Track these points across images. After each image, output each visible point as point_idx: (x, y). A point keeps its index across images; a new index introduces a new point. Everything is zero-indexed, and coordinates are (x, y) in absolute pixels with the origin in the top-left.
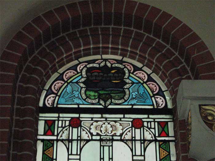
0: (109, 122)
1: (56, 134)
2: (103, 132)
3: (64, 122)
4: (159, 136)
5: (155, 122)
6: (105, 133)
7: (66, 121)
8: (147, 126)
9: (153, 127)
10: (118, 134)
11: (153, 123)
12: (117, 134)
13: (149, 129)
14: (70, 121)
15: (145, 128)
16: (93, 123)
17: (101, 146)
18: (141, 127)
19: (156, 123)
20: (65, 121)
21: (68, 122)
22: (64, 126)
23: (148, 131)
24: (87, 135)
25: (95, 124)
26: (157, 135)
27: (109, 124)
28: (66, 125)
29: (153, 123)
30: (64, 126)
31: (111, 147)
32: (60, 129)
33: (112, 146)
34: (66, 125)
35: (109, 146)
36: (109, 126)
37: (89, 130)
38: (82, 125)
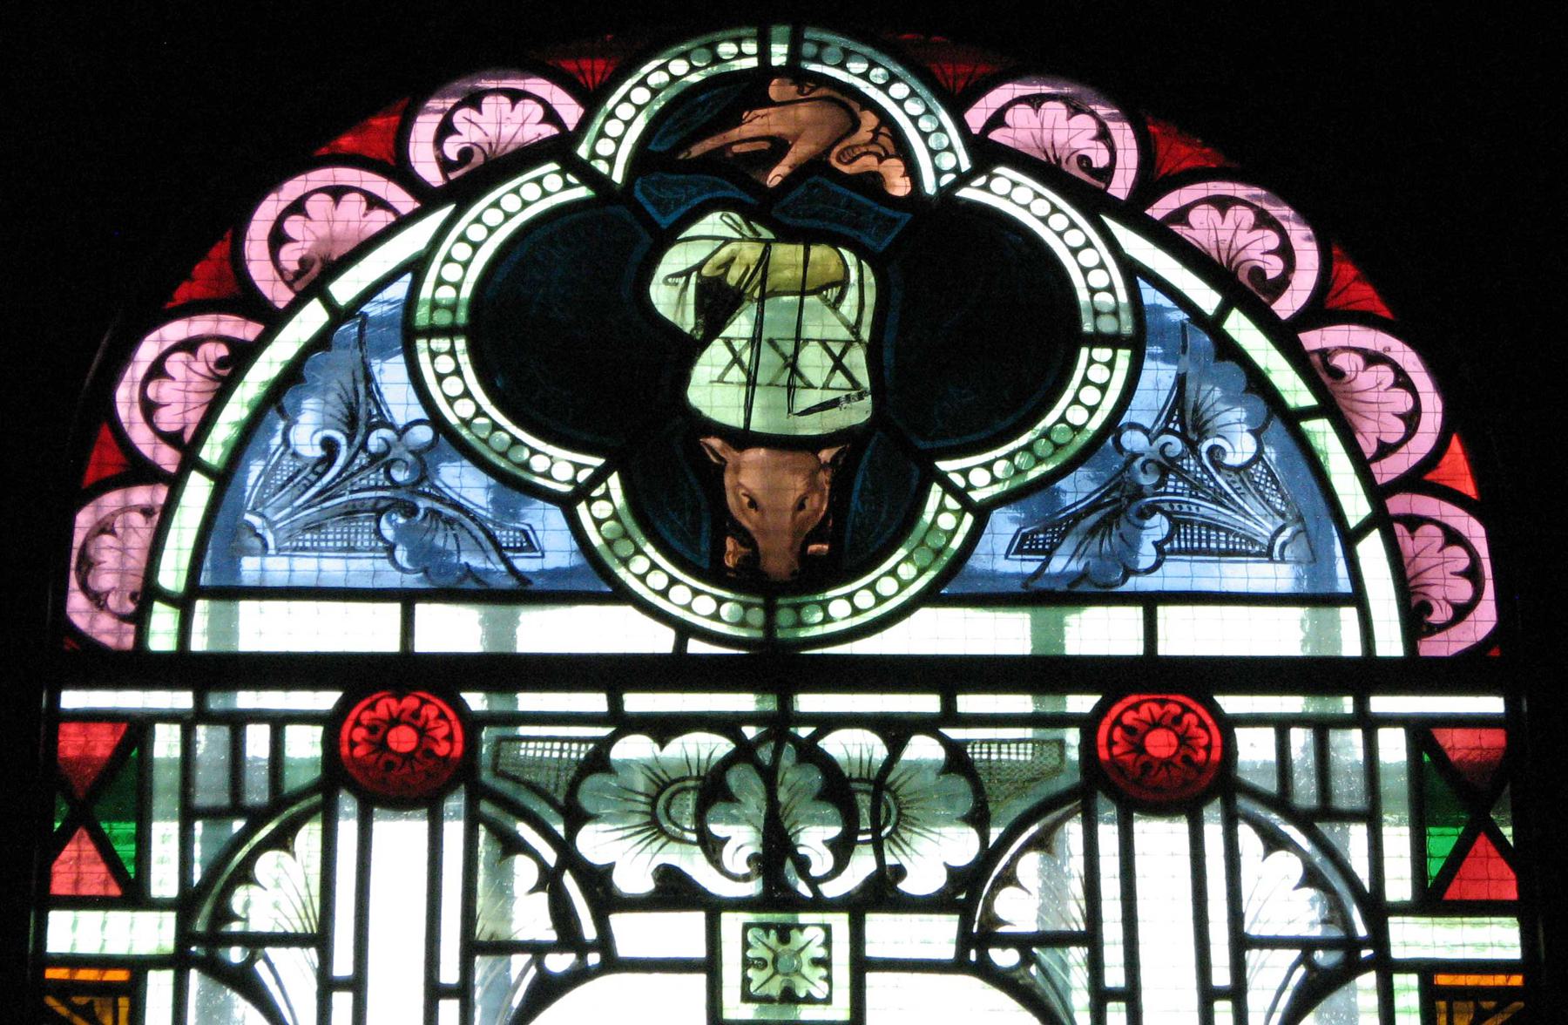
0: (804, 732)
1: (164, 881)
7: (292, 732)
8: (1270, 785)
10: (923, 878)
12: (907, 886)
13: (1306, 821)
14: (331, 723)
15: (1243, 803)
18: (1205, 799)
20: (278, 722)
26: (1399, 888)
38: (486, 776)
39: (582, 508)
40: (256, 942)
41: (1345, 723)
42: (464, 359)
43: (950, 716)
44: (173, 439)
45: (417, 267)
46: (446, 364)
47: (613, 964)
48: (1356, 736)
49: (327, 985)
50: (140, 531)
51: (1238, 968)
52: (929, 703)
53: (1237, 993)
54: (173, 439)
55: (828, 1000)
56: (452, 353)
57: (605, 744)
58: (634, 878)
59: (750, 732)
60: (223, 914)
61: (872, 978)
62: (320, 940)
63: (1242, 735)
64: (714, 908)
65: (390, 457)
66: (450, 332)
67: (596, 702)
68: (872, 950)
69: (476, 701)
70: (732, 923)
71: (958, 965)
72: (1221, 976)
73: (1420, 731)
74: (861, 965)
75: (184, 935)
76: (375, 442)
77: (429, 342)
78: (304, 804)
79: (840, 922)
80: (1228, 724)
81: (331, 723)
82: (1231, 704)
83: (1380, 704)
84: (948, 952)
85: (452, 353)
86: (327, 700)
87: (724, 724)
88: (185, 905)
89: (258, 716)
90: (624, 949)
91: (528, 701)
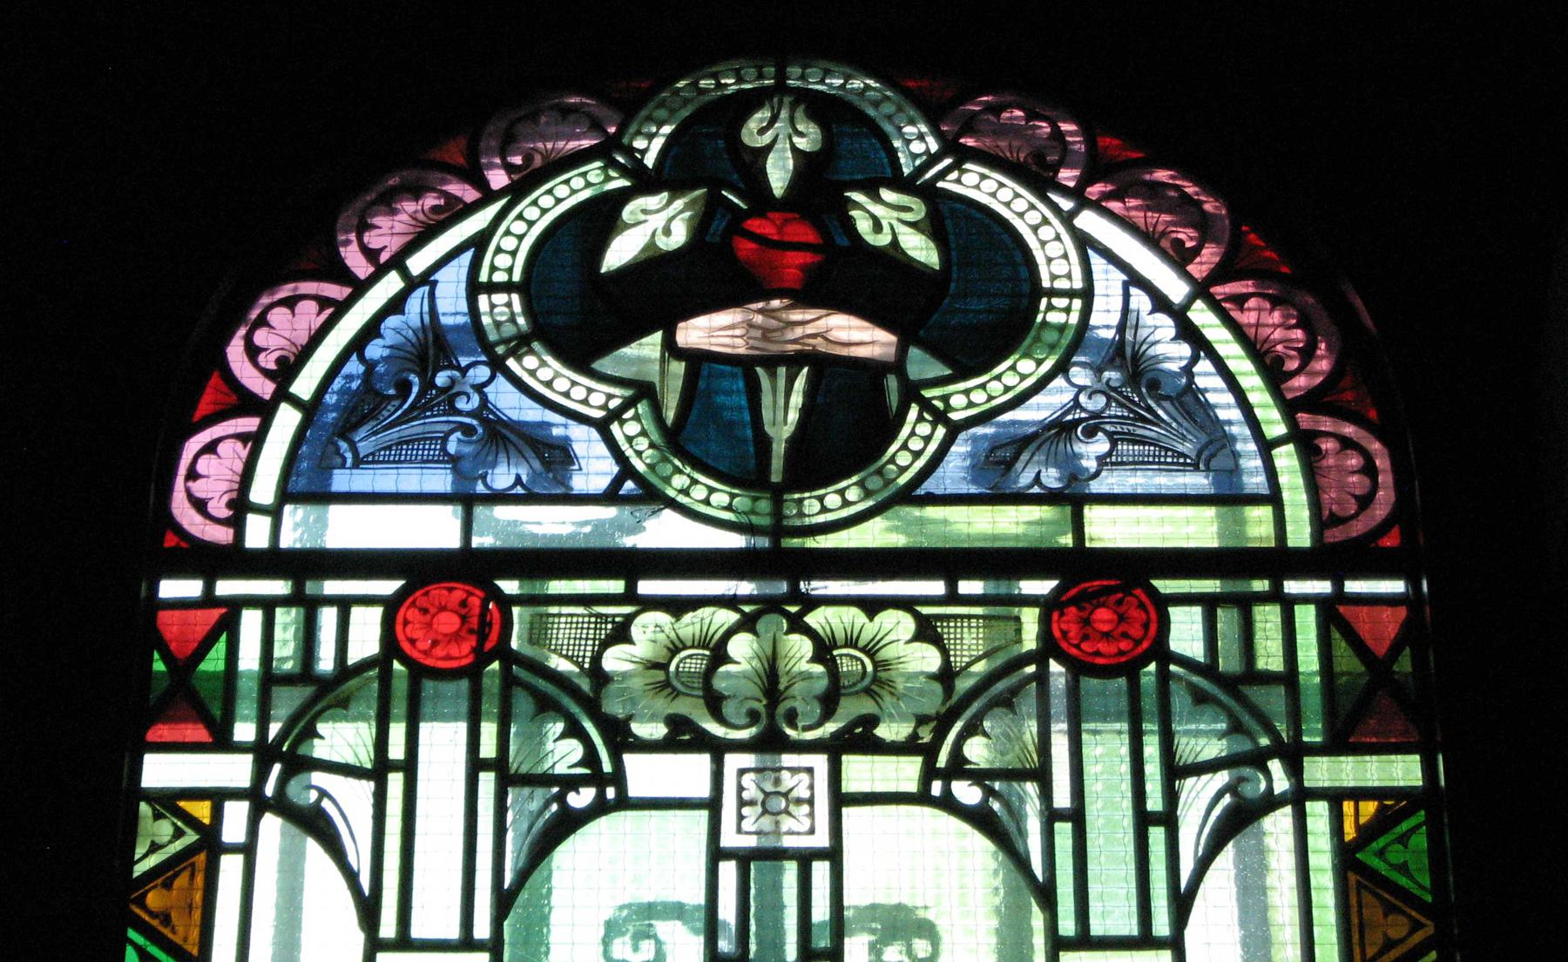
1: (244, 731)
3: (328, 618)
4: (1337, 745)
5: (1288, 604)
6: (754, 717)
7: (357, 612)
9: (1270, 657)
11: (1268, 618)
14: (391, 605)
17: (716, 854)
19: (1306, 617)
20: (344, 604)
21: (377, 612)
28: (353, 657)
30: (326, 662)
31: (821, 870)
32: (286, 702)
33: (834, 854)
34: (353, 657)
35: (805, 859)
39: (615, 428)
41: (1263, 598)
45: (479, 243)
47: (624, 803)
50: (232, 454)
51: (1171, 797)
53: (1169, 820)
59: (747, 609)
61: (848, 813)
63: (1176, 613)
65: (454, 391)
67: (616, 586)
68: (849, 785)
69: (510, 587)
71: (922, 798)
72: (1155, 803)
73: (1328, 609)
74: (840, 800)
76: (441, 379)
79: (820, 762)
82: (1165, 586)
83: (1292, 587)
84: (912, 787)
86: (388, 587)
87: (730, 602)
90: (635, 790)
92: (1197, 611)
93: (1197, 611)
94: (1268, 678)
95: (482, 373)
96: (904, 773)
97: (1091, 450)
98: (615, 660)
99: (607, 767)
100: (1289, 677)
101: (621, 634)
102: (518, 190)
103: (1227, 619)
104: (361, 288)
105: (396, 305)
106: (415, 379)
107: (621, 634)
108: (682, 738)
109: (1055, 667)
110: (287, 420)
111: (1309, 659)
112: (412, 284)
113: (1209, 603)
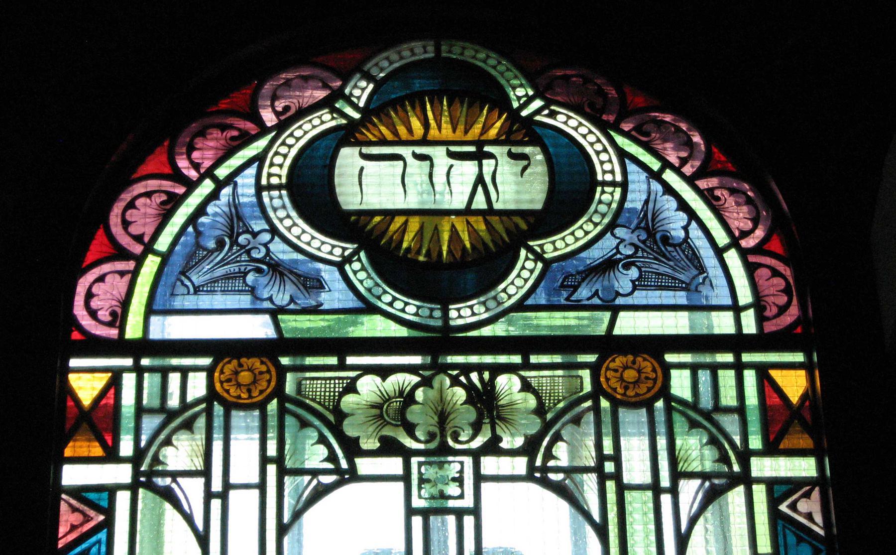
1: (126, 448)
2: (419, 434)
3: (174, 379)
4: (771, 449)
5: (739, 367)
6: (431, 437)
9: (729, 398)
11: (727, 378)
16: (354, 380)
19: (750, 377)
20: (185, 372)
22: (174, 402)
23: (705, 428)
24: (323, 451)
25: (369, 386)
26: (756, 443)
27: (455, 382)
29: (727, 378)
36: (460, 394)
37: (331, 418)
39: (347, 267)
40: (174, 475)
41: (726, 366)
42: (287, 200)
43: (526, 365)
44: (138, 239)
45: (260, 159)
46: (277, 202)
48: (731, 373)
49: (209, 495)
52: (517, 359)
54: (138, 239)
55: (461, 497)
56: (281, 197)
57: (354, 380)
58: (370, 444)
59: (427, 373)
60: (156, 460)
62: (206, 473)
63: (674, 373)
64: (407, 454)
66: (279, 187)
69: (285, 361)
70: (415, 461)
73: (762, 371)
75: (136, 473)
77: (269, 192)
78: (197, 409)
79: (468, 461)
80: (667, 368)
81: (210, 371)
82: (670, 358)
85: (281, 197)
88: (136, 460)
89: (175, 369)
91: (310, 361)
92: (687, 373)
93: (687, 373)
94: (728, 410)
95: (266, 237)
96: (519, 465)
97: (624, 280)
98: (349, 401)
99: (344, 464)
100: (741, 410)
101: (351, 388)
102: (281, 127)
103: (704, 376)
104: (191, 186)
105: (214, 196)
106: (227, 240)
107: (351, 388)
108: (389, 447)
109: (605, 404)
110: (151, 264)
111: (752, 398)
112: (220, 185)
113: (694, 368)
